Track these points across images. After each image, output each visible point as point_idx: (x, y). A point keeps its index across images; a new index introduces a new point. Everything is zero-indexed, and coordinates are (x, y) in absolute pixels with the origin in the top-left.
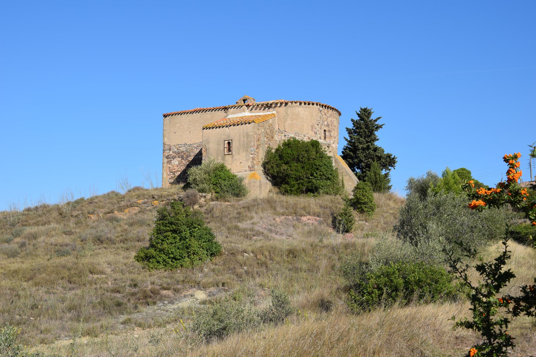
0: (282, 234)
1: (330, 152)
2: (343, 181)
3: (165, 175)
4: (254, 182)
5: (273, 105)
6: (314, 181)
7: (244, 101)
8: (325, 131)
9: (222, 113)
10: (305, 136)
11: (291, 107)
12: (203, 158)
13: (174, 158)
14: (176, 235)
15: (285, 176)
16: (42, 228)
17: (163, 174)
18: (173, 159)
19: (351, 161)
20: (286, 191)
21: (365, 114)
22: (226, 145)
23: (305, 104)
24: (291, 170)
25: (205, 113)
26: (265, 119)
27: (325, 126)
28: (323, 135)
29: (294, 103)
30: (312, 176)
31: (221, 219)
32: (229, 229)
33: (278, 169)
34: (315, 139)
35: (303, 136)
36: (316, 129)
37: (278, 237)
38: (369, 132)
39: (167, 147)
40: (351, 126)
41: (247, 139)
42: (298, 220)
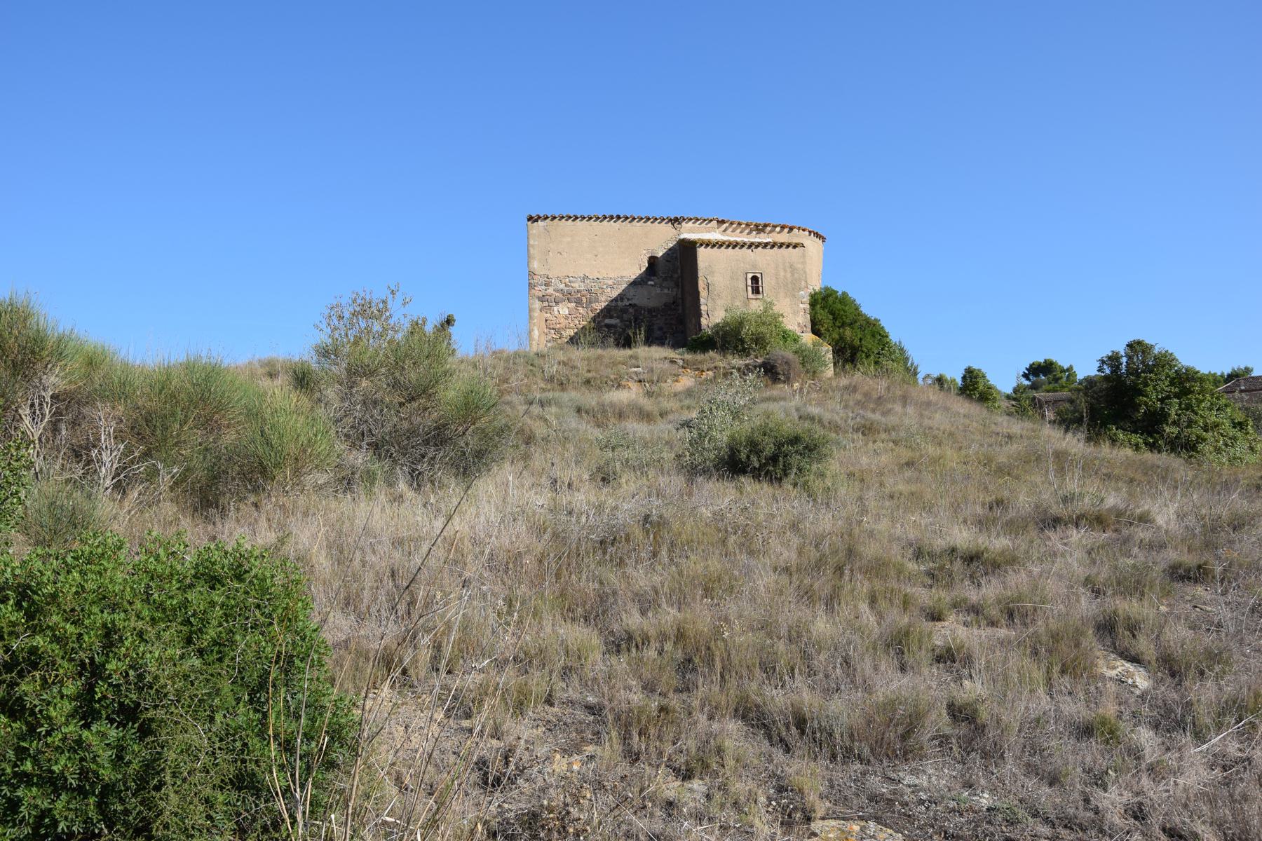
3: (536, 333)
12: (702, 301)
18: (557, 303)
22: (749, 282)
25: (629, 225)
41: (793, 275)
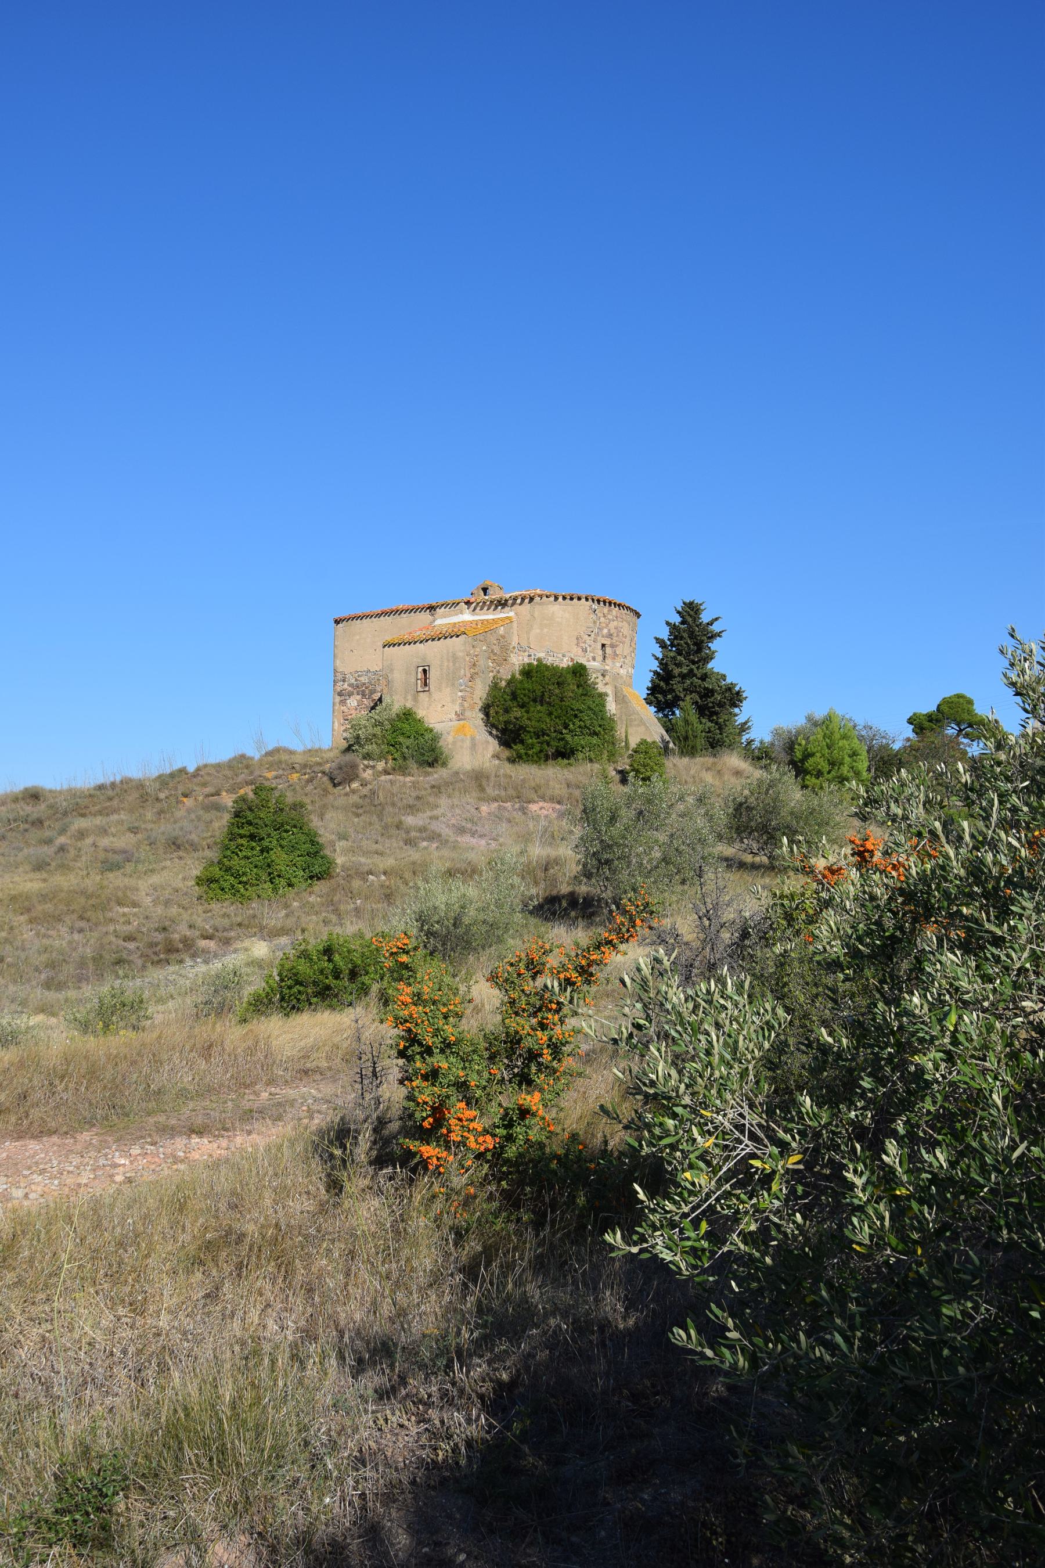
0: (481, 836)
1: (606, 684)
2: (626, 737)
3: (336, 724)
4: (462, 741)
5: (510, 602)
6: (568, 738)
7: (485, 590)
8: (603, 645)
9: (426, 616)
10: (564, 656)
11: (539, 604)
13: (350, 694)
14: (254, 844)
15: (519, 730)
16: (98, 821)
17: (333, 723)
19: (660, 697)
20: (520, 757)
21: (691, 610)
22: (420, 675)
23: (564, 598)
24: (529, 719)
26: (489, 628)
28: (600, 652)
29: (544, 598)
30: (566, 728)
31: (383, 809)
32: (386, 827)
33: (505, 718)
34: (583, 661)
35: (560, 655)
36: (585, 642)
37: (474, 841)
38: (695, 644)
39: (340, 677)
40: (665, 634)
41: (454, 664)
42: (523, 810)
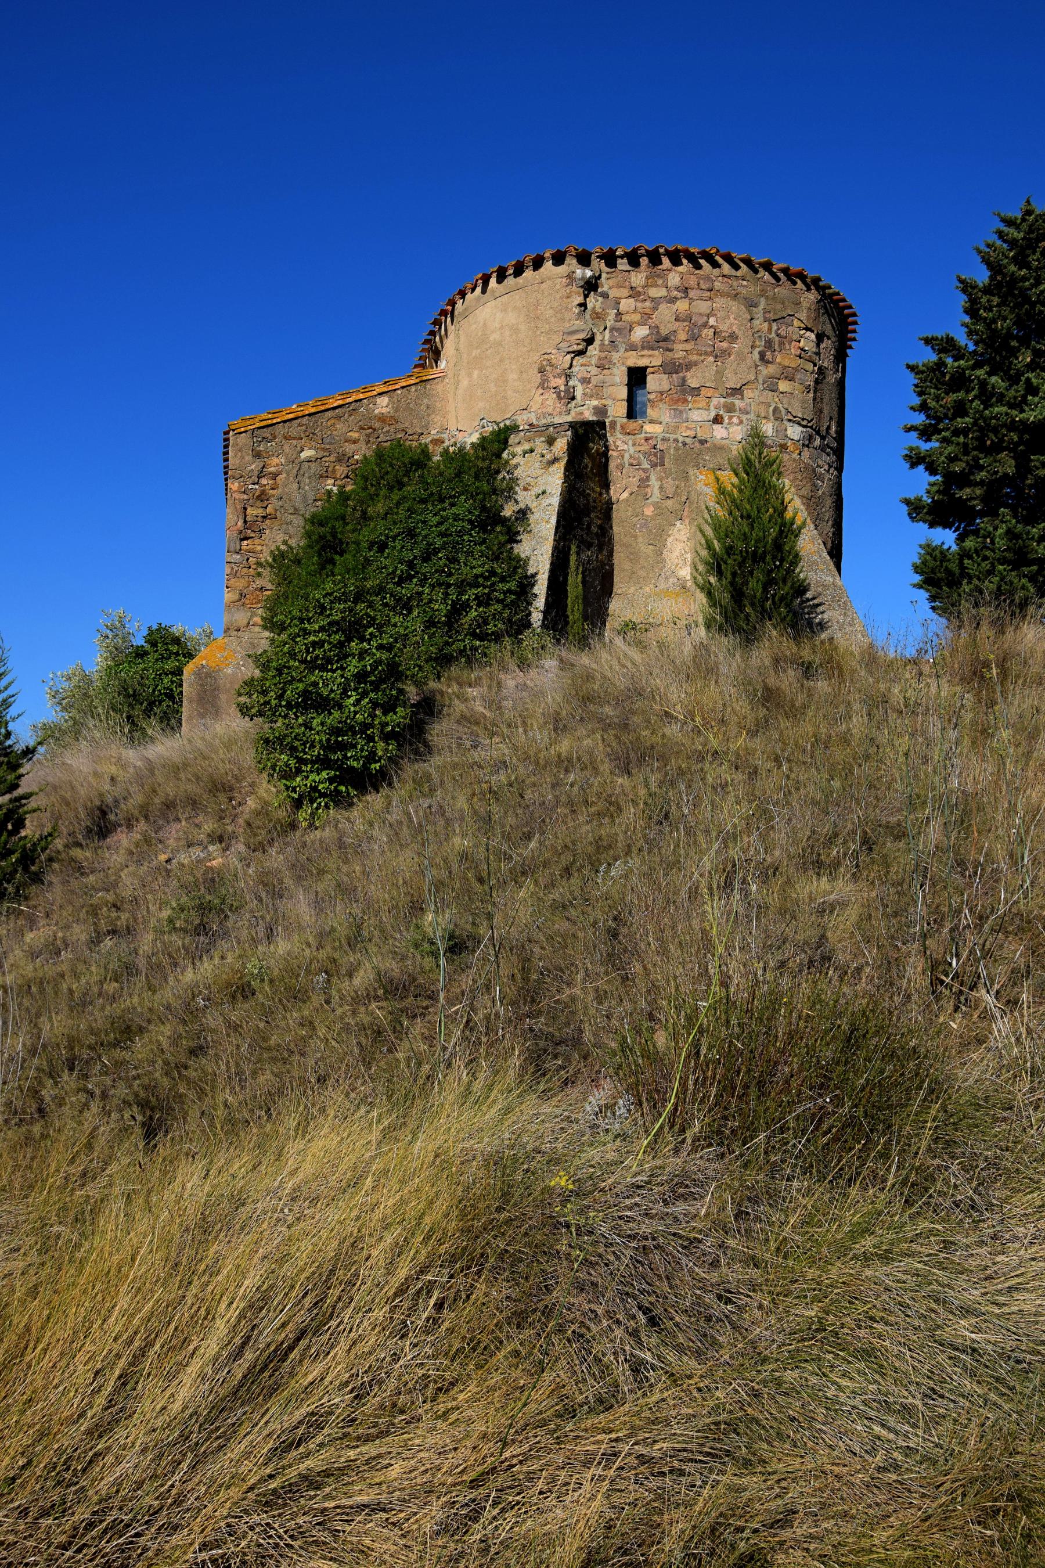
27: (632, 348)
